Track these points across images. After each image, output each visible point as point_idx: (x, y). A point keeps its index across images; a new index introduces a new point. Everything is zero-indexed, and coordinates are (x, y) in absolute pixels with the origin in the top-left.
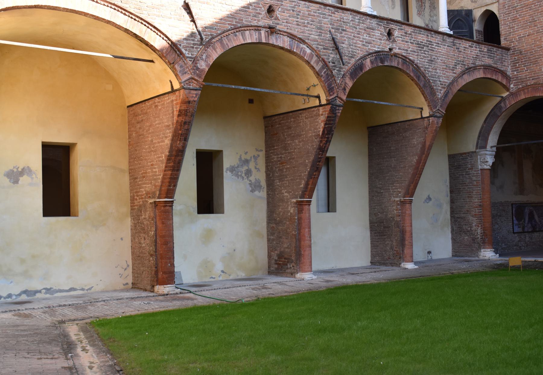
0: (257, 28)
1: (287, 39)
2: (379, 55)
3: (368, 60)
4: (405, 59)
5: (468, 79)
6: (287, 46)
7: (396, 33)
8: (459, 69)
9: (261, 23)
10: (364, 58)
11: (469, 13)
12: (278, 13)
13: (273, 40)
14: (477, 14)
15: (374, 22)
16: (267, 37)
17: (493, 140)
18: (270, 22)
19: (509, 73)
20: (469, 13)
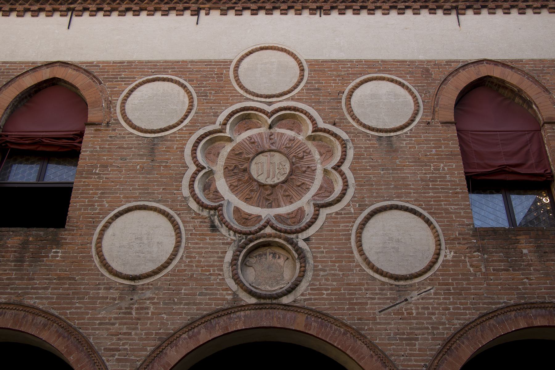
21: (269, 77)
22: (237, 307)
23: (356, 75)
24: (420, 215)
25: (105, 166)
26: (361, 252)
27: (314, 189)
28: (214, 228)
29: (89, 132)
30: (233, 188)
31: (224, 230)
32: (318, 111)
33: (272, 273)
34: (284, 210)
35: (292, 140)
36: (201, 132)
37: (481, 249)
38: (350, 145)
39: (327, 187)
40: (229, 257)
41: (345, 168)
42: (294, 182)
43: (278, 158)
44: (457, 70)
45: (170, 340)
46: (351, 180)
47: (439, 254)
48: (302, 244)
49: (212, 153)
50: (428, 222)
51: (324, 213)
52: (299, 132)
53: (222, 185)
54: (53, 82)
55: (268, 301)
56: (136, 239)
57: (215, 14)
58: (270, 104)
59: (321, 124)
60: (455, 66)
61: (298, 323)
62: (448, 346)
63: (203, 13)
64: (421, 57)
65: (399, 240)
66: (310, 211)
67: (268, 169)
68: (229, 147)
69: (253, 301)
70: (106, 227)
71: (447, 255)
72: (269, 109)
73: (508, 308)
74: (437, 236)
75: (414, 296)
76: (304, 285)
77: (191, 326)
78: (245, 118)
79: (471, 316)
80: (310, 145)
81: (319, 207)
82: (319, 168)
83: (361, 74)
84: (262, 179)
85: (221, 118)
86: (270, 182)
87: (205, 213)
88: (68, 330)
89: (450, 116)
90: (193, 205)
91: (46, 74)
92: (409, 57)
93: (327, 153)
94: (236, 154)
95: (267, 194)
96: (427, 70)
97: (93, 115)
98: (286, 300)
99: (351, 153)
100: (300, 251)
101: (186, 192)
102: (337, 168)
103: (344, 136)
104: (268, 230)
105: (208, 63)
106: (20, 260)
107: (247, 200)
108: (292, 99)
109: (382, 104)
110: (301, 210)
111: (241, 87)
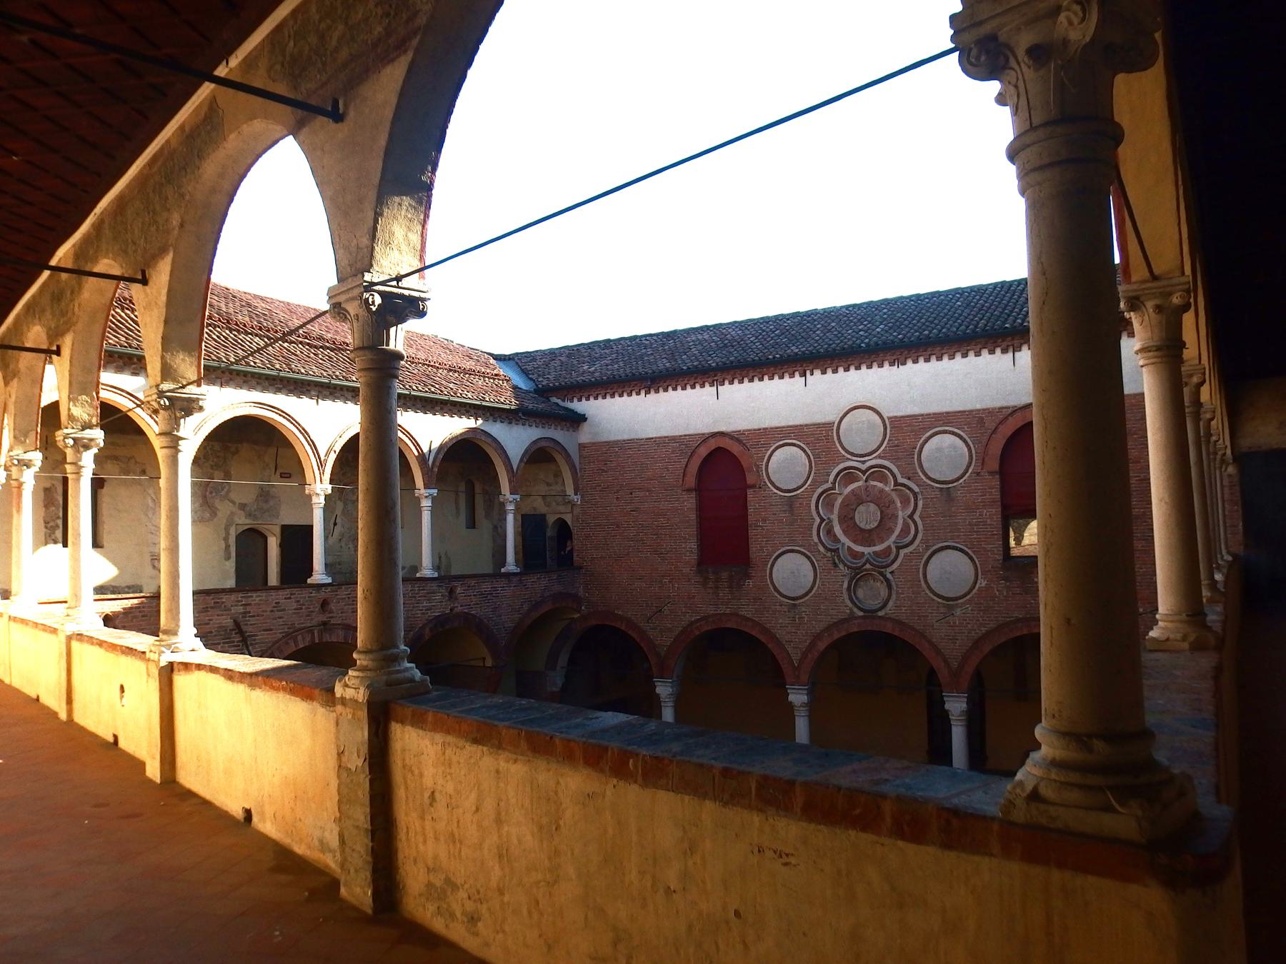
0: (310, 631)
1: (341, 633)
2: (441, 620)
3: (427, 630)
4: (466, 617)
5: (535, 615)
6: (341, 639)
7: (459, 590)
8: (526, 607)
9: (314, 622)
10: (424, 626)
11: (543, 516)
12: (332, 606)
13: (327, 638)
14: (551, 519)
15: (434, 586)
16: (321, 638)
17: (563, 660)
18: (323, 618)
19: (581, 593)
20: (543, 516)
21: (862, 436)
22: (852, 617)
23: (926, 429)
24: (967, 554)
25: (764, 520)
26: (926, 582)
27: (897, 533)
28: (835, 565)
29: (750, 492)
30: (845, 532)
31: (841, 566)
32: (898, 467)
33: (872, 593)
34: (878, 548)
35: (882, 491)
36: (820, 490)
37: (1006, 579)
38: (920, 497)
39: (906, 530)
40: (845, 585)
41: (916, 517)
42: (883, 527)
43: (872, 507)
44: (1006, 418)
45: (818, 637)
46: (920, 527)
47: (975, 583)
48: (889, 576)
49: (829, 505)
50: (971, 558)
51: (902, 552)
52: (886, 483)
53: (838, 530)
54: (719, 449)
55: (870, 614)
56: (792, 572)
57: (817, 373)
58: (864, 462)
59: (901, 480)
60: (1006, 412)
61: (889, 628)
62: (977, 643)
63: (808, 373)
64: (978, 406)
65: (951, 570)
66: (894, 550)
67: (867, 516)
68: (840, 500)
69: (861, 614)
70: (773, 565)
71: (982, 583)
72: (864, 467)
73: (1018, 620)
74: (976, 569)
75: (958, 612)
76: (891, 603)
77: (828, 628)
78: (848, 476)
79: (992, 625)
80: (894, 495)
81: (898, 548)
82: (900, 513)
83: (931, 428)
84: (862, 525)
85: (831, 478)
86: (868, 527)
87: (829, 554)
88: (765, 631)
89: (995, 465)
90: (821, 549)
91: (713, 444)
92: (968, 407)
93: (905, 502)
94: (843, 505)
95: (865, 537)
96: (982, 419)
97: (750, 479)
98: (880, 614)
99: (920, 503)
100: (887, 580)
101: (816, 540)
102: (911, 516)
103: (916, 489)
104: (868, 566)
105: (818, 426)
106: (730, 587)
107: (854, 542)
108: (879, 457)
109: (945, 454)
110: (889, 547)
111: (844, 448)
